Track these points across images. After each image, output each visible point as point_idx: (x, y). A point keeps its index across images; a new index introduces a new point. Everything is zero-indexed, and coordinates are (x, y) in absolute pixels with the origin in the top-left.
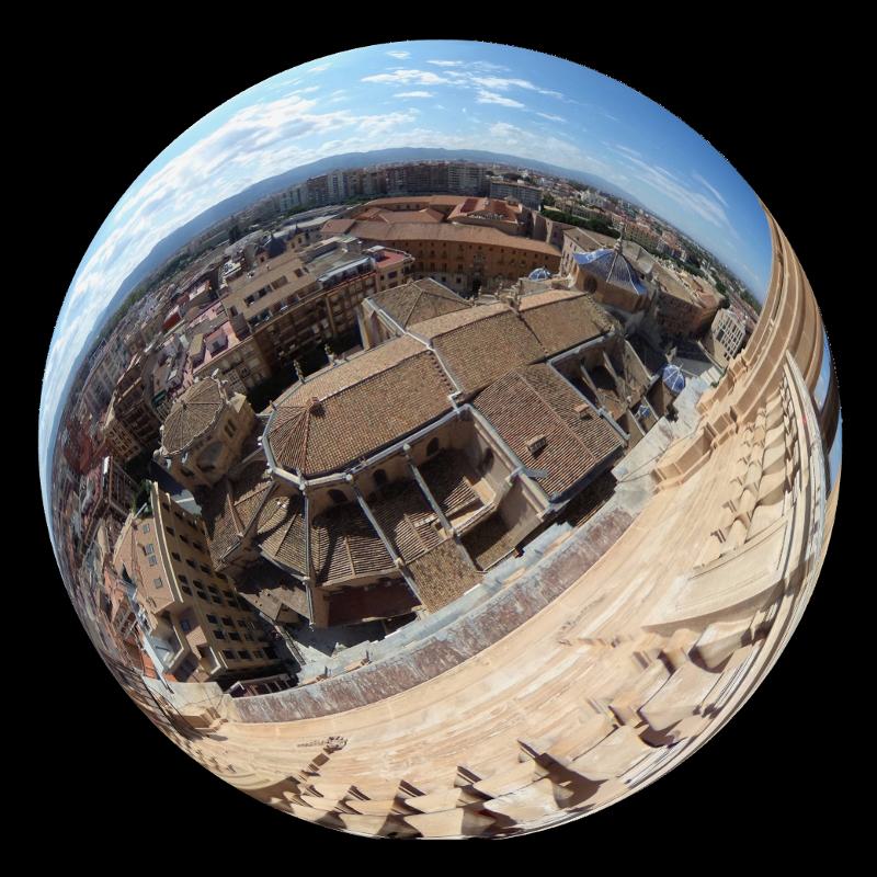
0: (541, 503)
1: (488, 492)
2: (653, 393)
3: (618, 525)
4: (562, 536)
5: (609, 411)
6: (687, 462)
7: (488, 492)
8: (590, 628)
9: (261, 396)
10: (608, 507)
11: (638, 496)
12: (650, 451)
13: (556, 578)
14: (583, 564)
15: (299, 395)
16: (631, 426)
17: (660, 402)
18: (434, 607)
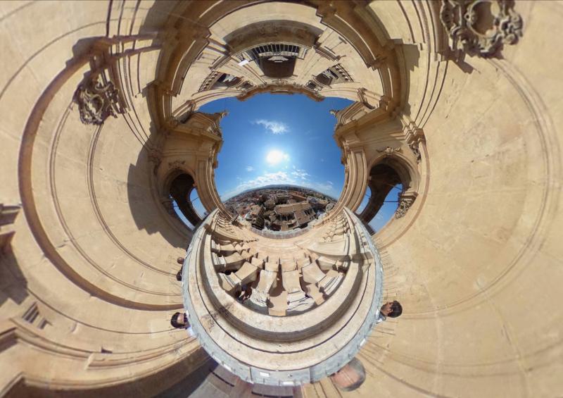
0: (298, 225)
1: (293, 221)
2: (315, 216)
3: (307, 231)
4: (299, 229)
5: (309, 217)
6: (319, 225)
7: (293, 221)
8: (299, 244)
9: (277, 204)
10: (306, 228)
11: (311, 228)
12: (313, 223)
13: (297, 234)
14: (301, 234)
15: (280, 206)
16: (312, 219)
17: (316, 217)
18: (283, 230)
